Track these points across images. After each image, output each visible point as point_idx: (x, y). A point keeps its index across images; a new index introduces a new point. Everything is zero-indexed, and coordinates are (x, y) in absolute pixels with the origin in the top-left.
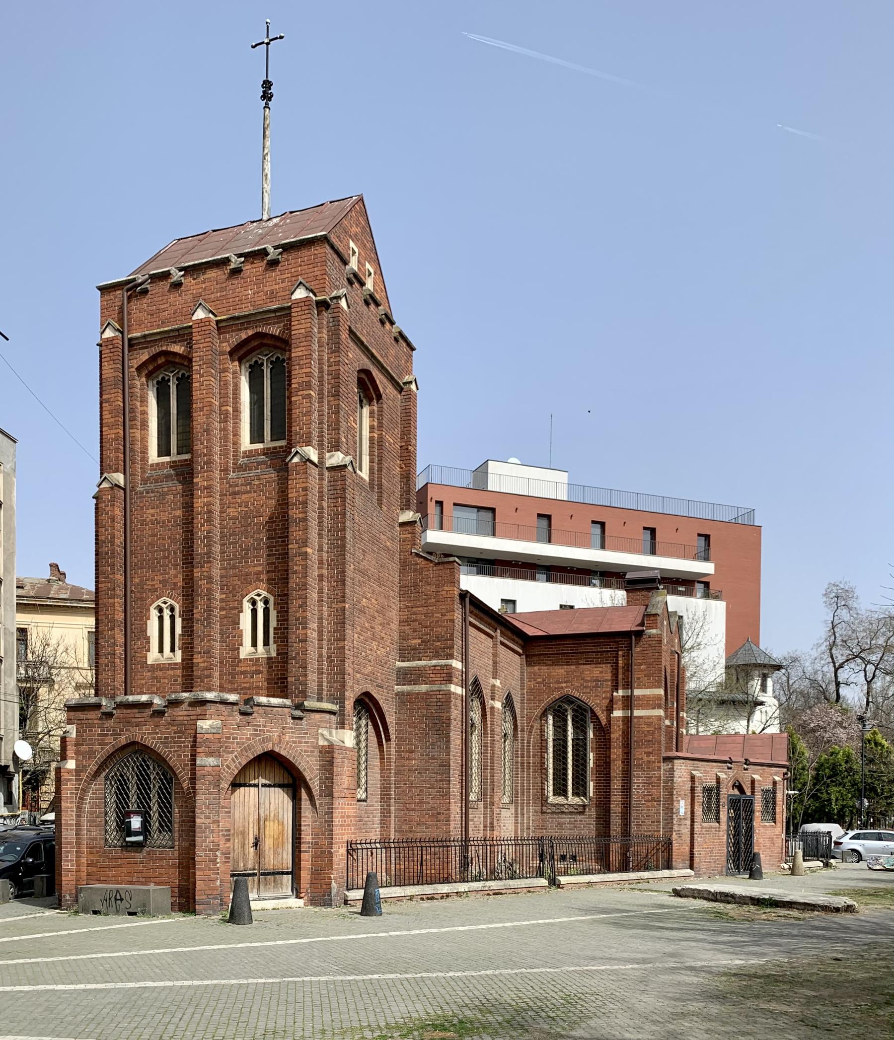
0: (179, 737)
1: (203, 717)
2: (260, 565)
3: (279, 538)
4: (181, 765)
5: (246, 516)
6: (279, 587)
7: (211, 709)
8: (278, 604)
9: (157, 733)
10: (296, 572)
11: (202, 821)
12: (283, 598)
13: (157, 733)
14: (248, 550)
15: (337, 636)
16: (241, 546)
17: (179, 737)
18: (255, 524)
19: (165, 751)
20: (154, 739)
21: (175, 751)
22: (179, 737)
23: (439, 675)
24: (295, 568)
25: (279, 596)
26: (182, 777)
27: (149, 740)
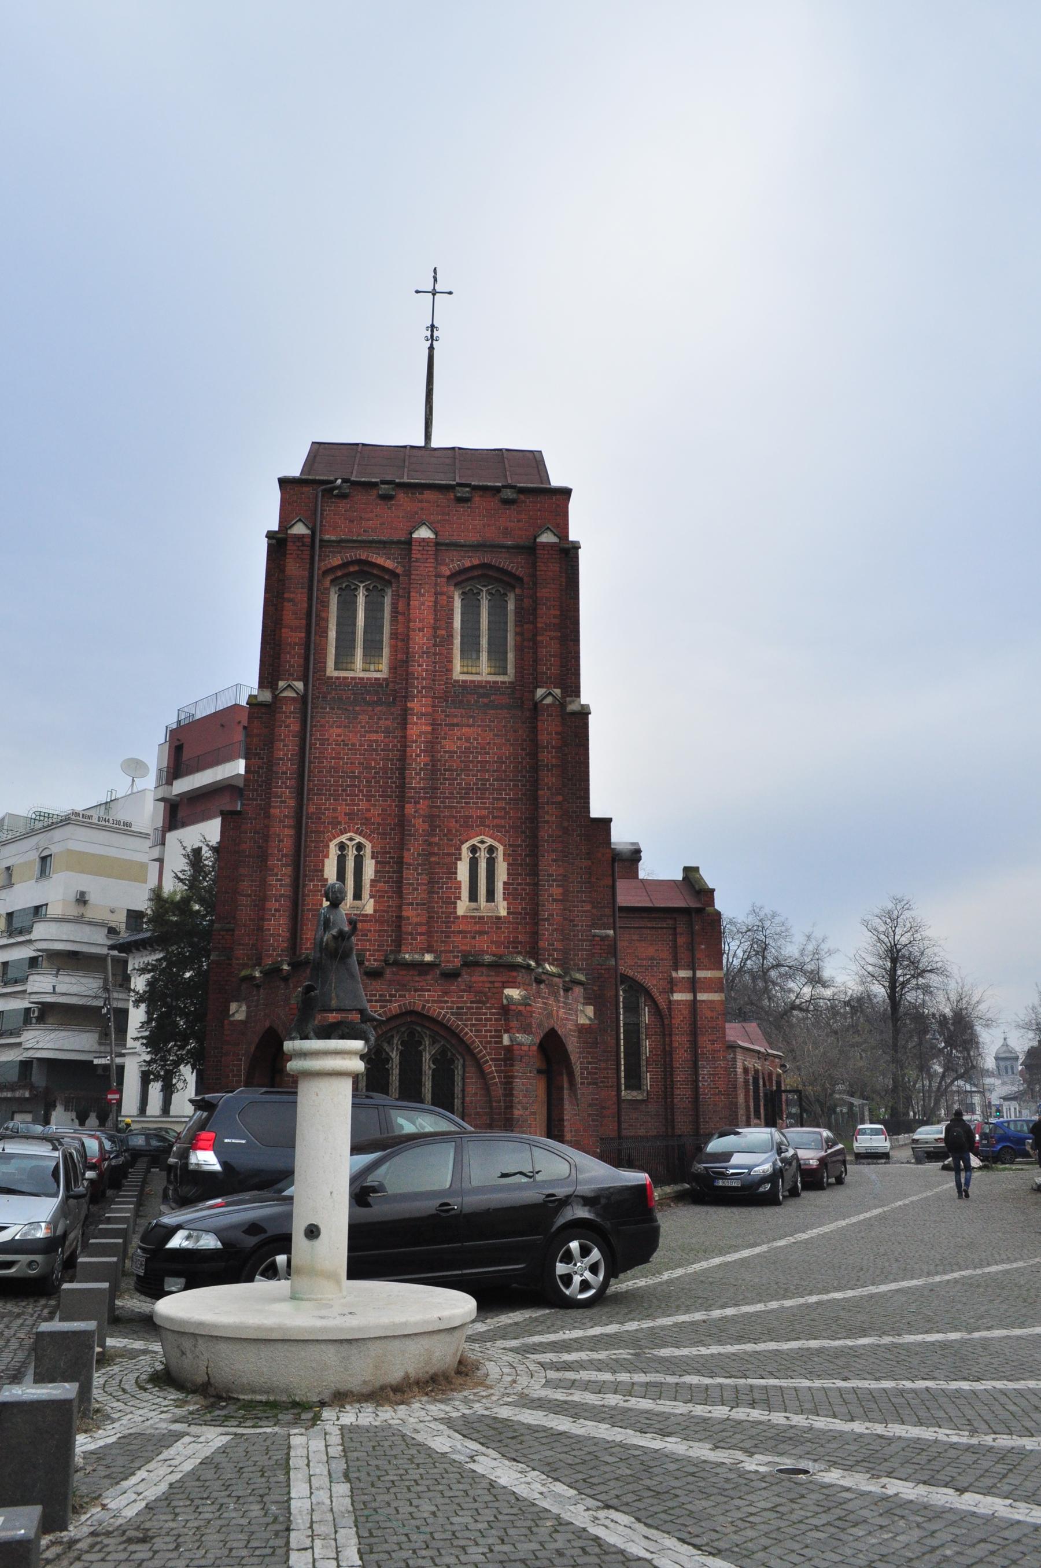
0: (477, 1008)
1: (506, 984)
2: (485, 808)
3: (510, 780)
4: (481, 1042)
5: (467, 751)
6: (510, 836)
7: (521, 976)
8: (509, 855)
9: (446, 1002)
10: (547, 822)
11: (521, 1112)
12: (516, 849)
13: (446, 1002)
14: (468, 789)
15: (581, 897)
16: (459, 784)
17: (481, 1008)
18: (478, 762)
19: (458, 1025)
20: (442, 1008)
21: (473, 1025)
22: (477, 1008)
23: (599, 947)
24: (547, 818)
25: (510, 845)
26: (484, 1056)
27: (435, 1010)
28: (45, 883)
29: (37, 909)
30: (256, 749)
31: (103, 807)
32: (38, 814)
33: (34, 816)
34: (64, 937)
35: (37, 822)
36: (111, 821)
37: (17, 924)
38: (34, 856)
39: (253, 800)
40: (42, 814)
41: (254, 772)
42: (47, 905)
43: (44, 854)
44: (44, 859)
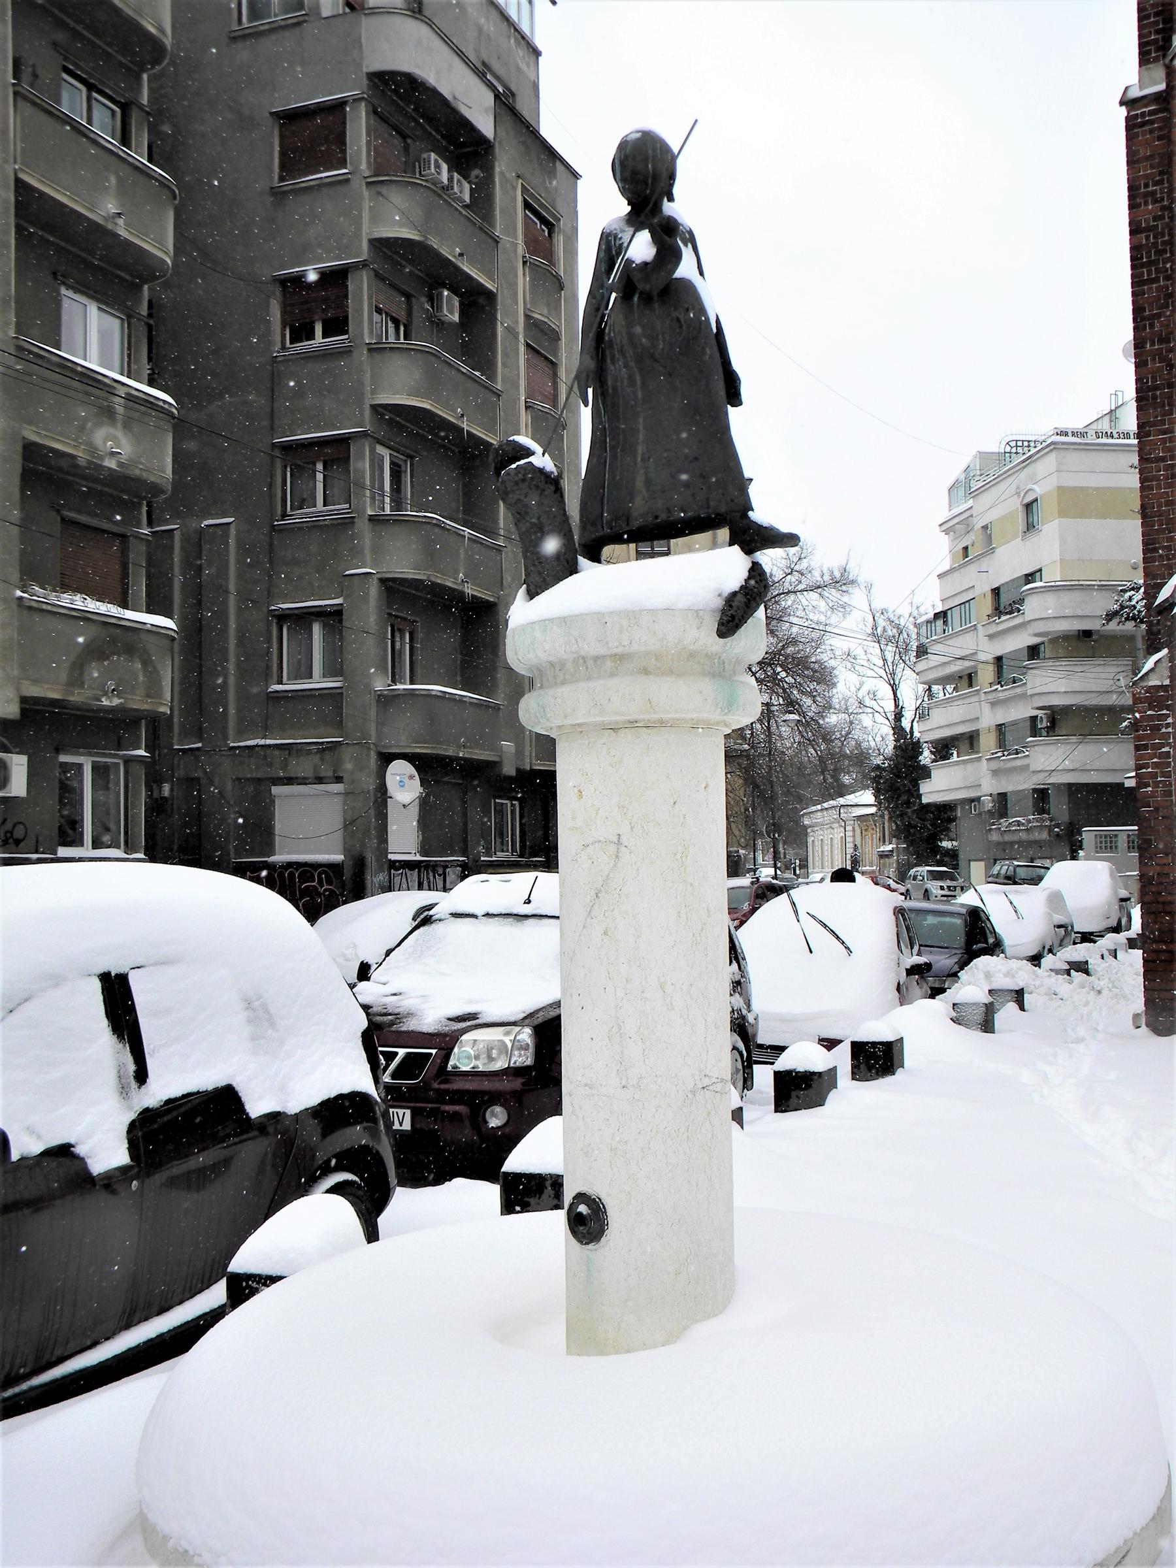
28: (1034, 540)
29: (1029, 577)
30: (1146, 186)
31: (1107, 418)
32: (1013, 444)
33: (1008, 449)
34: (1068, 612)
35: (1013, 455)
36: (1116, 435)
37: (1005, 599)
38: (1015, 505)
39: (1152, 281)
40: (1020, 444)
41: (1148, 229)
42: (1040, 570)
43: (1028, 499)
44: (1029, 507)
